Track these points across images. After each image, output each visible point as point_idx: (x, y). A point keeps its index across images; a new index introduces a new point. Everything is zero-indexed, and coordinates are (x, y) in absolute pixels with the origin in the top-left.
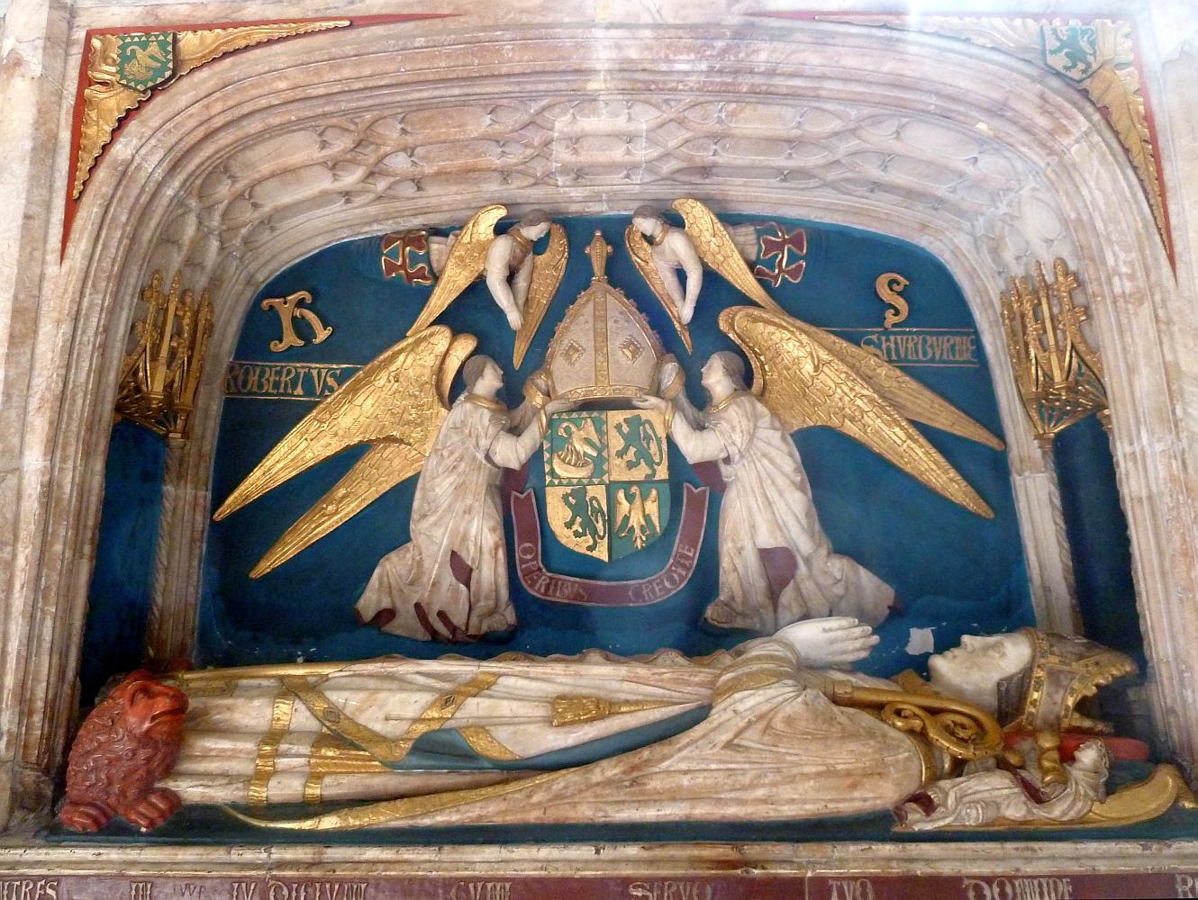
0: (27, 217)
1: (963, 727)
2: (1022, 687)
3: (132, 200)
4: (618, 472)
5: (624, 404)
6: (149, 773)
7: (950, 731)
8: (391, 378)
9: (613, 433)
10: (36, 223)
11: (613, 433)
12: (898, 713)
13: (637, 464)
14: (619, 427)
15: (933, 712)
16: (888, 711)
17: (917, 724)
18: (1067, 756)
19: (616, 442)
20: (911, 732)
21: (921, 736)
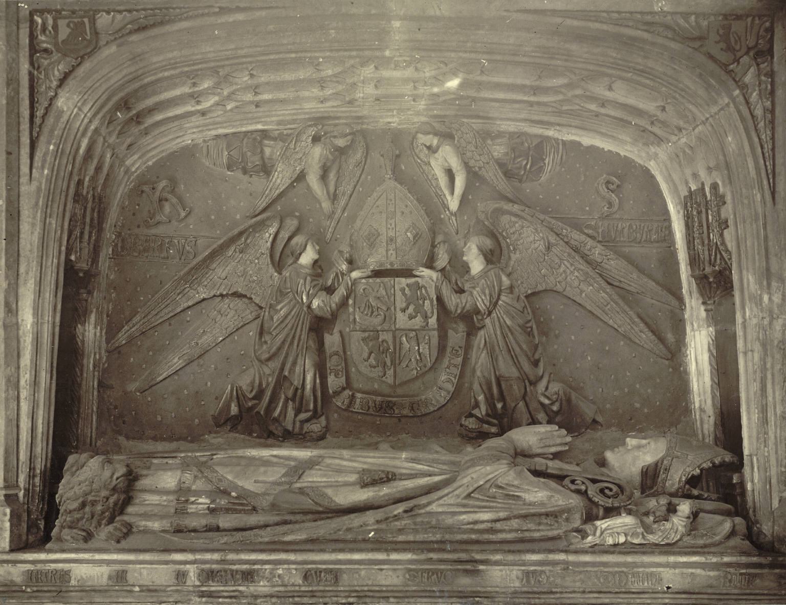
0: (9, 153)
1: (611, 490)
2: (656, 470)
3: (72, 137)
4: (402, 320)
5: (407, 273)
6: (114, 510)
7: (602, 491)
8: (237, 250)
9: (399, 294)
10: (13, 157)
11: (399, 294)
12: (573, 482)
13: (415, 317)
14: (403, 290)
15: (594, 481)
16: (567, 481)
17: (583, 488)
18: (672, 509)
19: (400, 303)
20: (578, 492)
21: (584, 494)
